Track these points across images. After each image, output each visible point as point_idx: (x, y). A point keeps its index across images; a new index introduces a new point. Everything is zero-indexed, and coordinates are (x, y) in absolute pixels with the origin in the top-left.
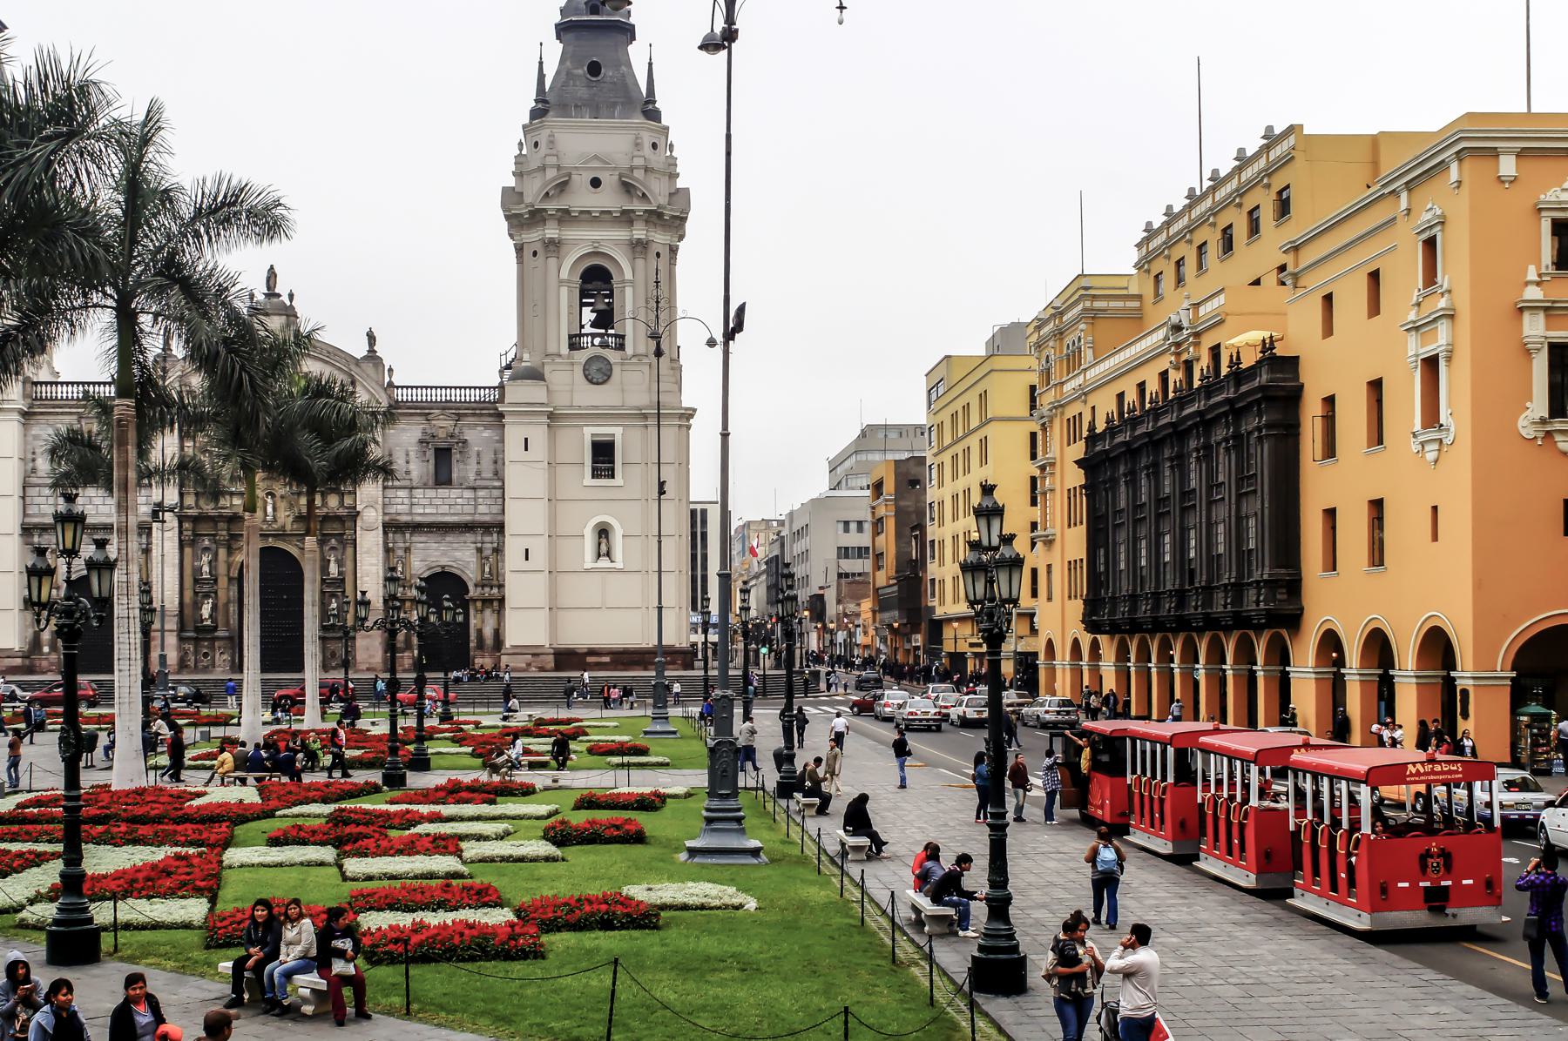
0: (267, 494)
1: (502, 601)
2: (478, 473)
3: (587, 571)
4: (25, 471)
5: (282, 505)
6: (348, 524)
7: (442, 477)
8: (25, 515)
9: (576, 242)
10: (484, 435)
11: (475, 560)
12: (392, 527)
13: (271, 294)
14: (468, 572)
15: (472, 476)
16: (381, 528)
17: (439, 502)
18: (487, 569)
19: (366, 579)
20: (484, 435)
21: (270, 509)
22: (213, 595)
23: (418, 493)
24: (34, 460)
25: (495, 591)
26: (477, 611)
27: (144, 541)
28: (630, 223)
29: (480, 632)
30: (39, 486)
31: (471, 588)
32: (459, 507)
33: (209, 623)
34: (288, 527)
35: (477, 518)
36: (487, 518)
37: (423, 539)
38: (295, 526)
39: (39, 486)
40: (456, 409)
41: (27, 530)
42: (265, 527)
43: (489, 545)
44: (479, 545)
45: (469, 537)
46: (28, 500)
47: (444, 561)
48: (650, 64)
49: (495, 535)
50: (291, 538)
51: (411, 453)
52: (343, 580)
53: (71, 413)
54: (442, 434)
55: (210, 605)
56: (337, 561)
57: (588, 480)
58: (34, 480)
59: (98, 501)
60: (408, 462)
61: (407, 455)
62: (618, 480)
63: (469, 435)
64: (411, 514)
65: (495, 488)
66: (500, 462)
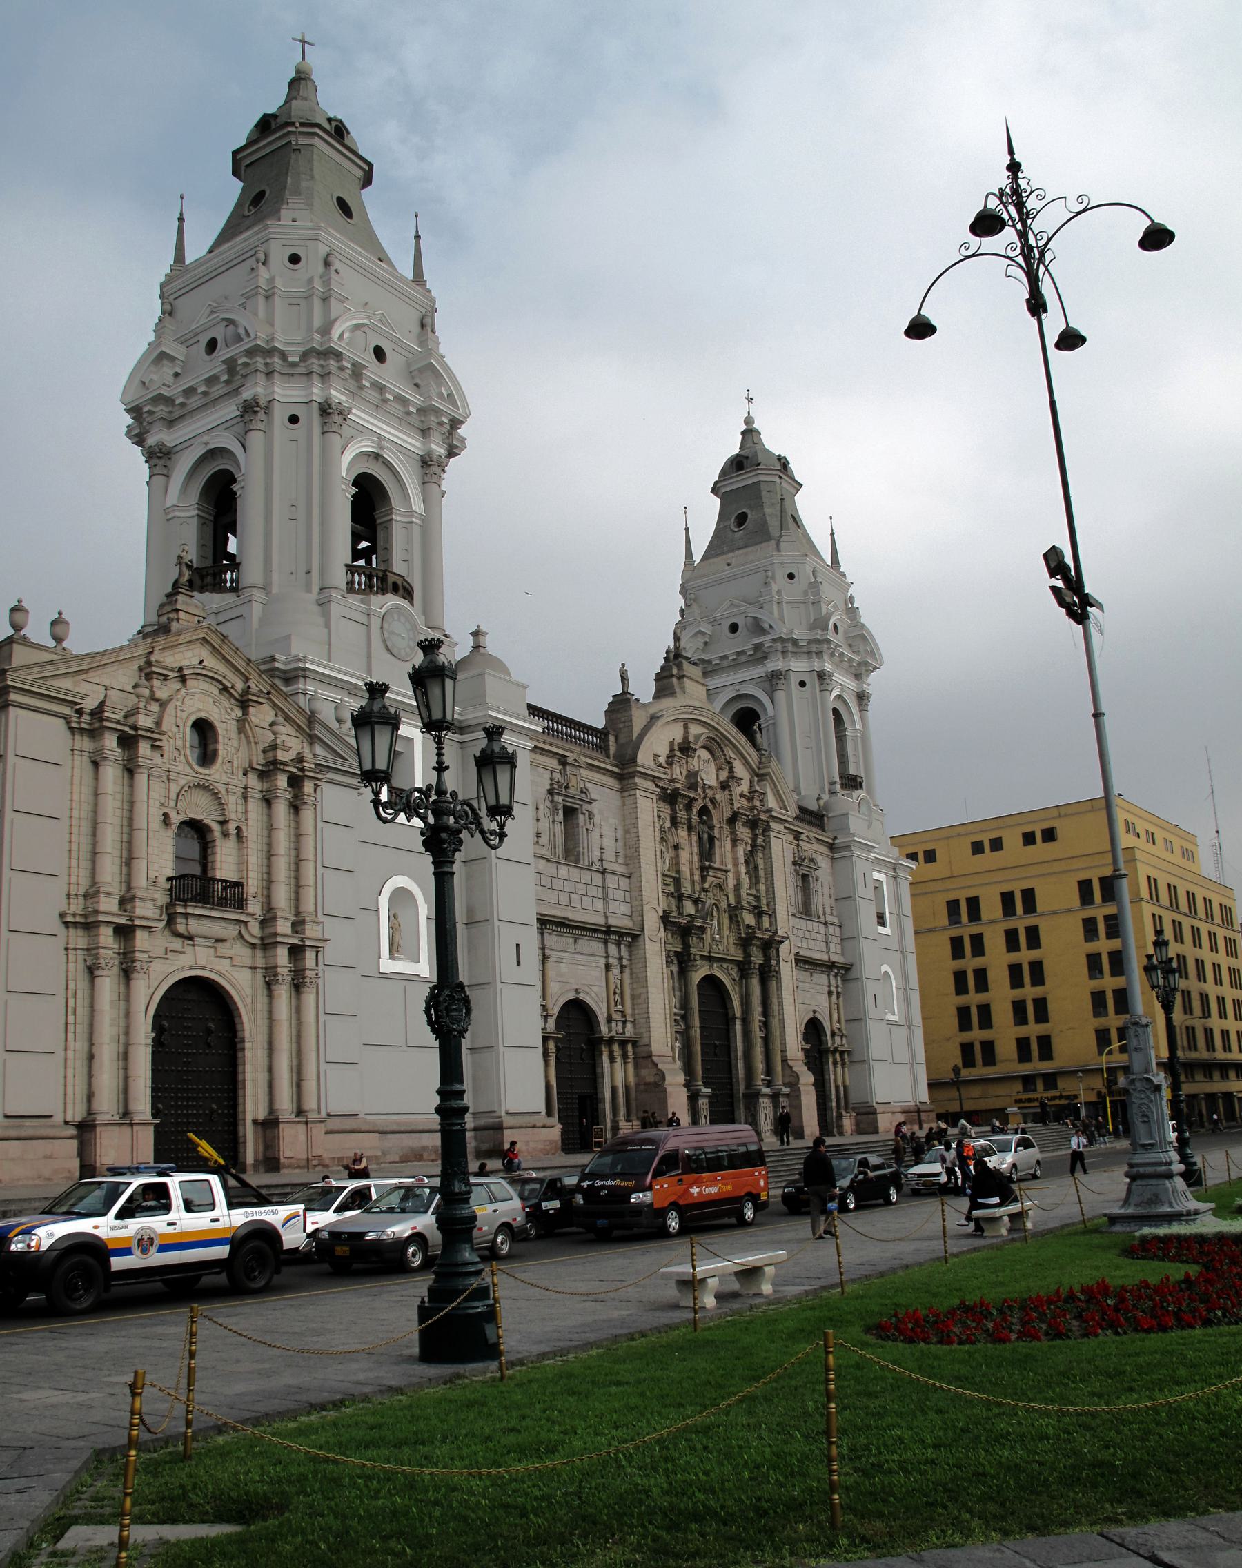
6: (772, 952)
48: (832, 534)
59: (581, 889)
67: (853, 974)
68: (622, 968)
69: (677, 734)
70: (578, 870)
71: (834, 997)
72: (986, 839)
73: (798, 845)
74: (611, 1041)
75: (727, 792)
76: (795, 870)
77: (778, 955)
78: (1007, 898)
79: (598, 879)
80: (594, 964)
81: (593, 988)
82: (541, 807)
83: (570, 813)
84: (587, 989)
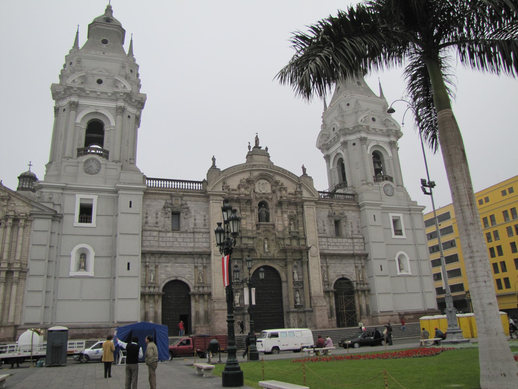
0: (266, 238)
1: (369, 291)
2: (352, 232)
3: (399, 276)
4: (142, 223)
5: (273, 244)
7: (338, 234)
8: (142, 246)
9: (371, 140)
10: (353, 215)
11: (355, 272)
12: (324, 256)
13: (257, 146)
14: (353, 278)
15: (350, 233)
16: (319, 256)
17: (338, 244)
18: (360, 276)
19: (314, 281)
20: (353, 215)
21: (266, 246)
22: (240, 291)
23: (330, 240)
24: (147, 217)
25: (366, 286)
26: (359, 296)
27: (205, 261)
28: (389, 136)
29: (360, 306)
30: (150, 231)
31: (355, 285)
32: (347, 247)
33: (239, 306)
34: (275, 256)
35: (356, 252)
36: (359, 252)
37: (334, 262)
38: (279, 255)
39: (150, 231)
40: (342, 202)
41: (144, 254)
42: (264, 255)
43: (360, 265)
44: (357, 265)
45: (352, 261)
46: (144, 238)
47: (343, 272)
48: (380, 84)
49: (362, 260)
50: (276, 261)
51: (325, 221)
52: (302, 283)
53: (167, 194)
54: (337, 213)
55: (239, 296)
56: (298, 273)
57: (394, 236)
58: (147, 228)
59: (180, 240)
60: (324, 226)
61: (323, 222)
62: (404, 236)
63: (346, 214)
64: (327, 249)
65: (360, 238)
66: (360, 227)
67: (369, 257)
68: (205, 267)
69: (246, 176)
70: (179, 233)
71: (360, 268)
72: (506, 188)
73: (332, 209)
74: (194, 295)
75: (275, 194)
76: (329, 219)
77: (308, 255)
78: (505, 213)
79: (191, 235)
80: (188, 266)
81: (187, 275)
82: (159, 213)
83: (176, 214)
84: (182, 276)
